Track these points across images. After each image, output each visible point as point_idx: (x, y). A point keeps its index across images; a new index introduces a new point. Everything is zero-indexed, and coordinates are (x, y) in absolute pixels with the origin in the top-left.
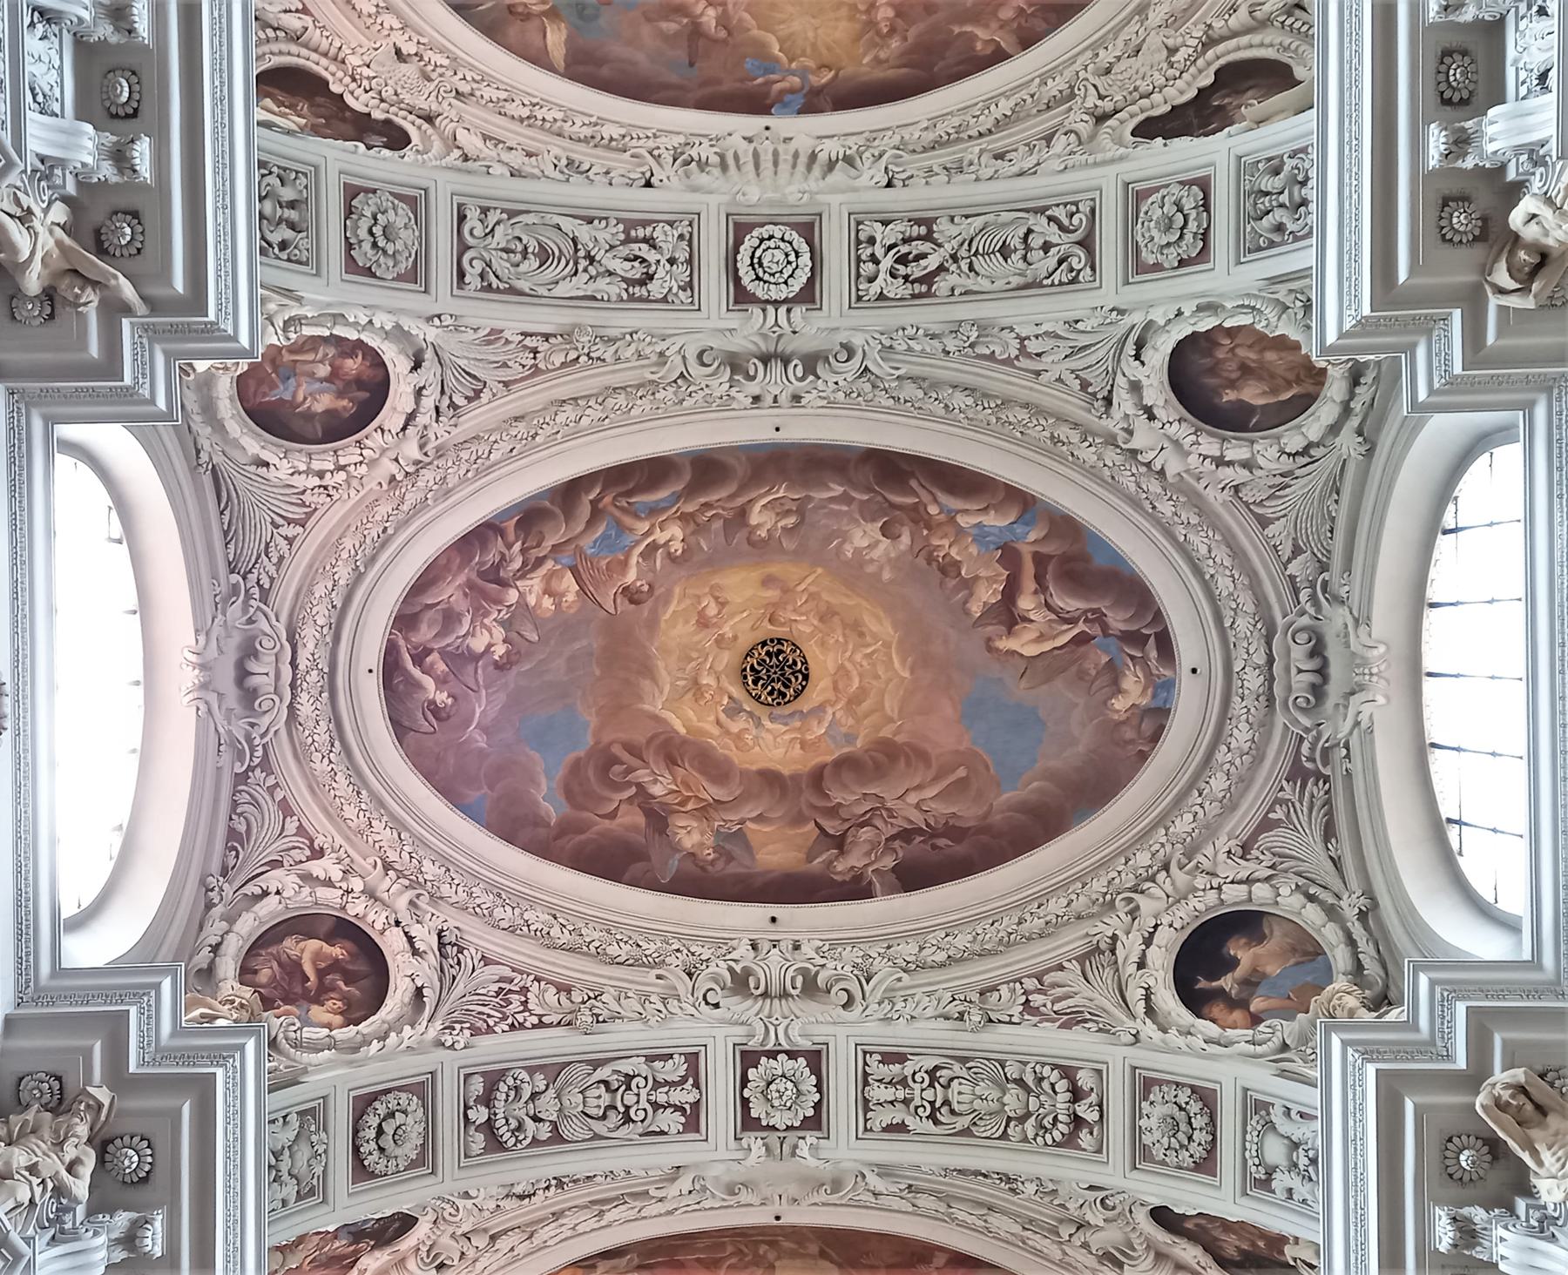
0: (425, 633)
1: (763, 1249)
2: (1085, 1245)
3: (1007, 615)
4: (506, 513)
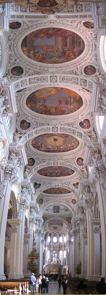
0: (77, 145)
2: (34, 119)
3: (41, 144)
4: (71, 150)
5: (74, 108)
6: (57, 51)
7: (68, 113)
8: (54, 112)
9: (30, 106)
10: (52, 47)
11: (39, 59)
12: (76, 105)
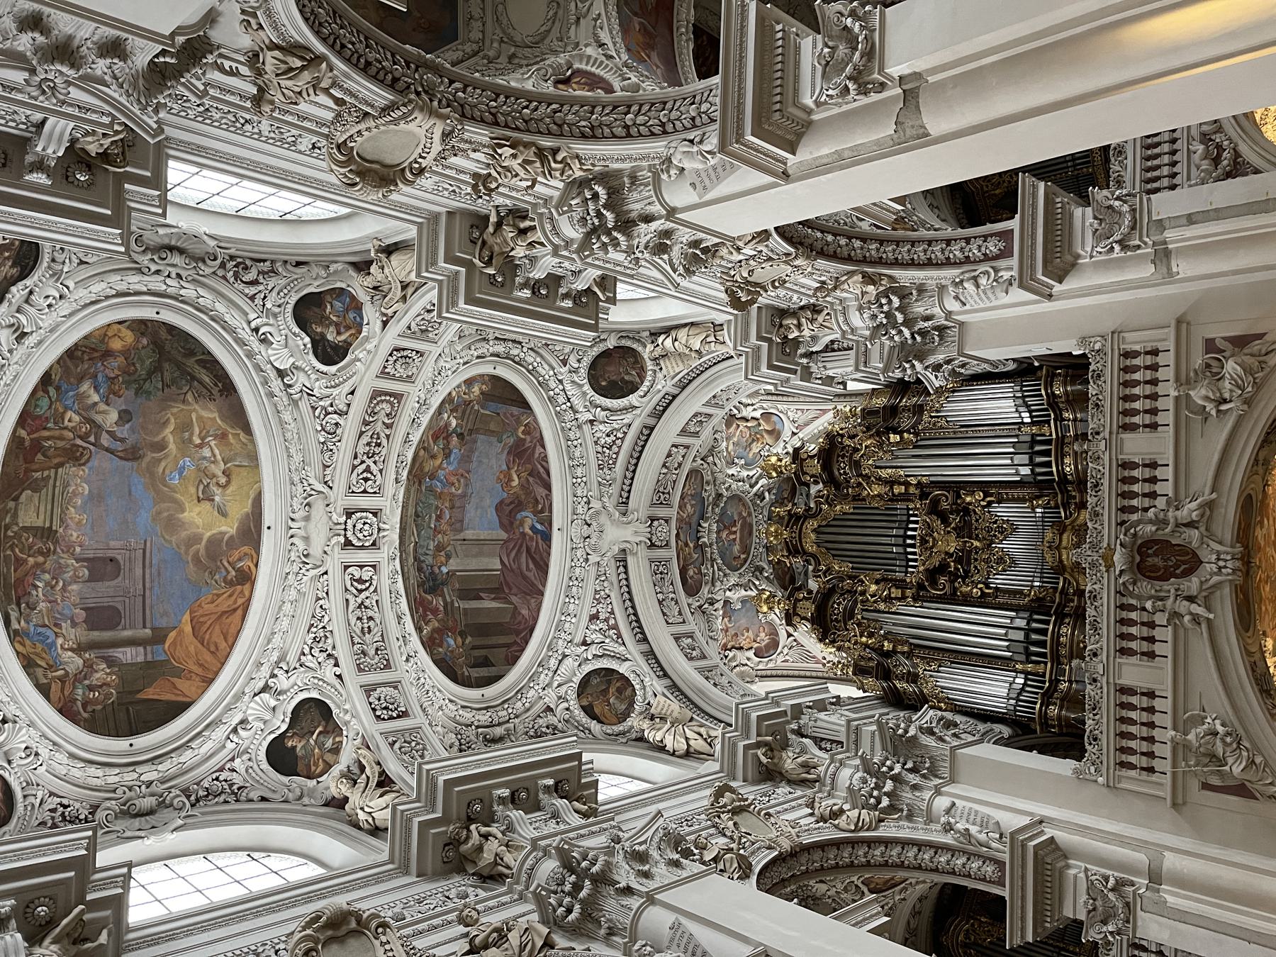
1: (10, 533)
2: (10, 351)
5: (62, 680)
6: (439, 548)
7: (16, 632)
8: (15, 516)
9: (116, 345)
10: (458, 525)
11: (422, 452)
12: (91, 688)
